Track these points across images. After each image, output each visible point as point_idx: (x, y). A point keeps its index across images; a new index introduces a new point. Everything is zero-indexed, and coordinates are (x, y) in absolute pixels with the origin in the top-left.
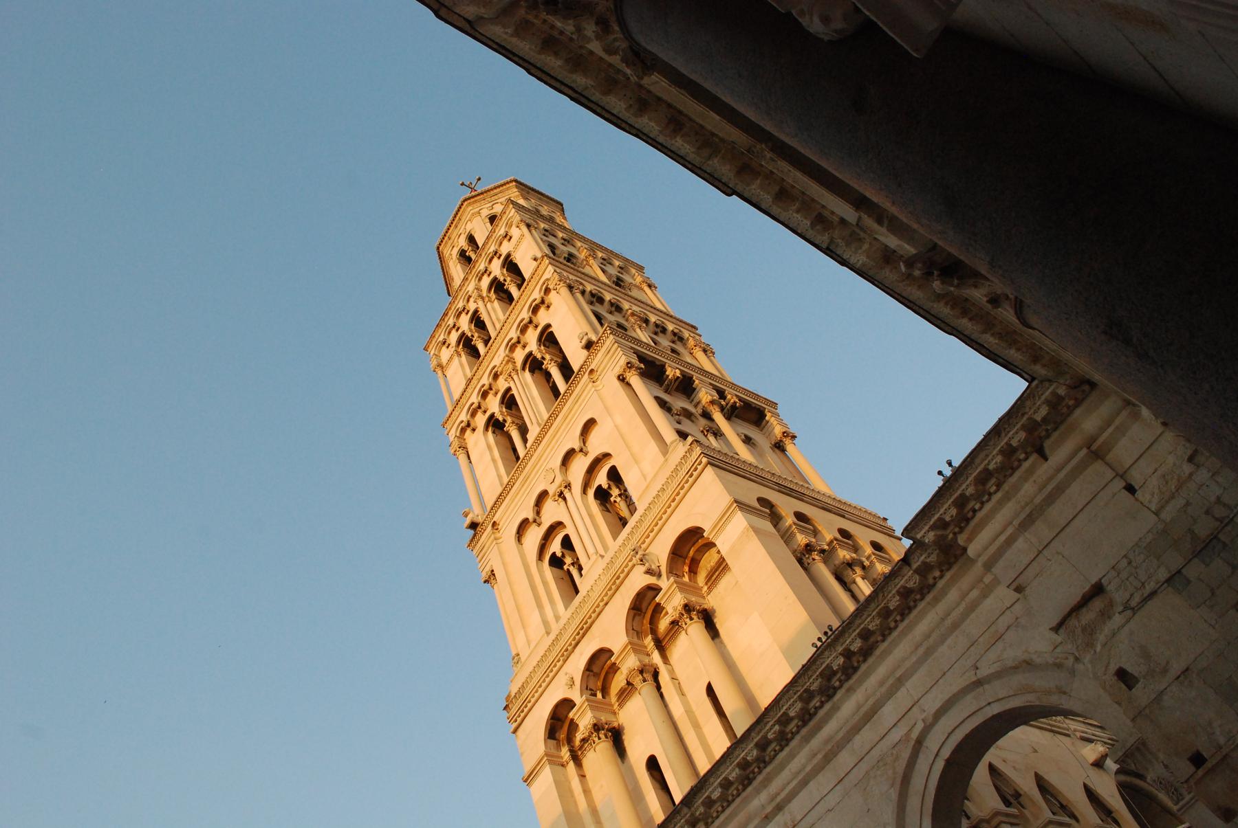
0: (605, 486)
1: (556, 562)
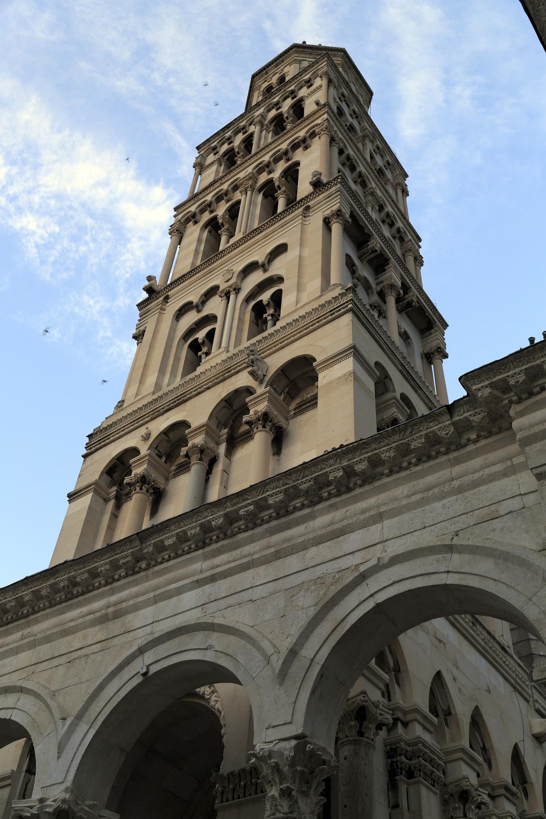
0: (265, 303)
1: (195, 347)
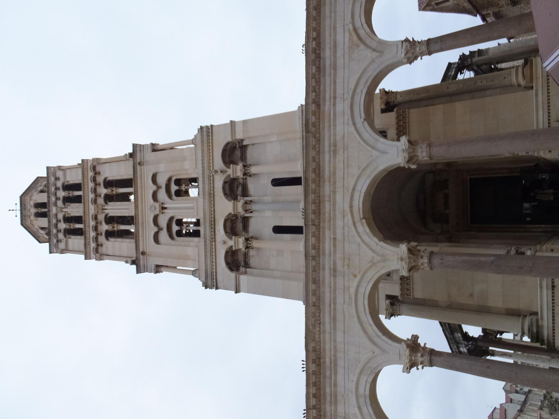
1: (179, 234)
